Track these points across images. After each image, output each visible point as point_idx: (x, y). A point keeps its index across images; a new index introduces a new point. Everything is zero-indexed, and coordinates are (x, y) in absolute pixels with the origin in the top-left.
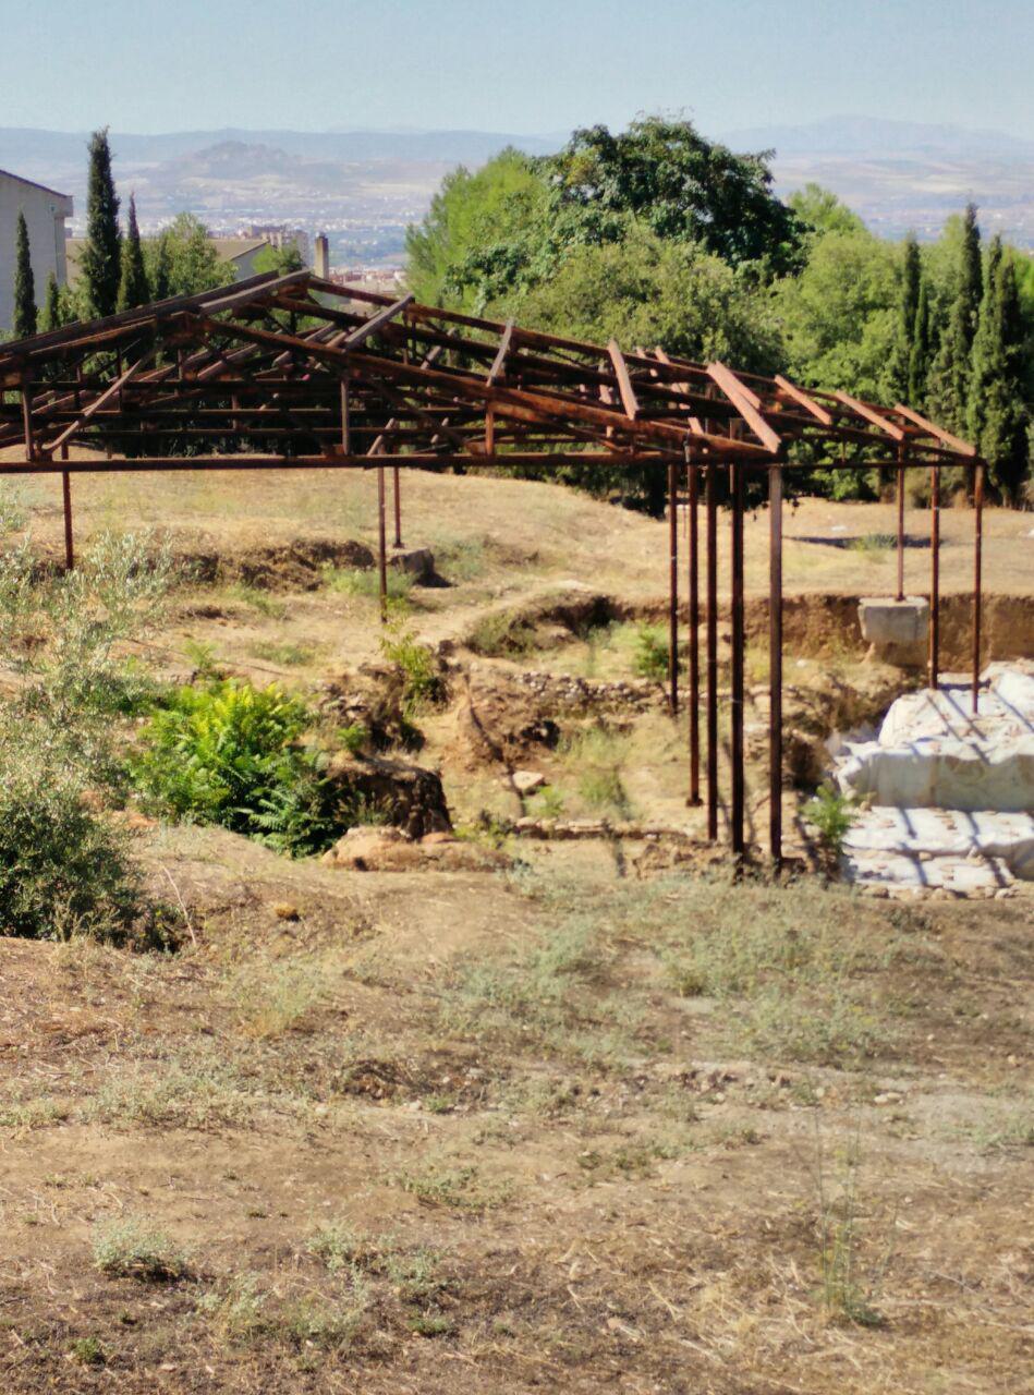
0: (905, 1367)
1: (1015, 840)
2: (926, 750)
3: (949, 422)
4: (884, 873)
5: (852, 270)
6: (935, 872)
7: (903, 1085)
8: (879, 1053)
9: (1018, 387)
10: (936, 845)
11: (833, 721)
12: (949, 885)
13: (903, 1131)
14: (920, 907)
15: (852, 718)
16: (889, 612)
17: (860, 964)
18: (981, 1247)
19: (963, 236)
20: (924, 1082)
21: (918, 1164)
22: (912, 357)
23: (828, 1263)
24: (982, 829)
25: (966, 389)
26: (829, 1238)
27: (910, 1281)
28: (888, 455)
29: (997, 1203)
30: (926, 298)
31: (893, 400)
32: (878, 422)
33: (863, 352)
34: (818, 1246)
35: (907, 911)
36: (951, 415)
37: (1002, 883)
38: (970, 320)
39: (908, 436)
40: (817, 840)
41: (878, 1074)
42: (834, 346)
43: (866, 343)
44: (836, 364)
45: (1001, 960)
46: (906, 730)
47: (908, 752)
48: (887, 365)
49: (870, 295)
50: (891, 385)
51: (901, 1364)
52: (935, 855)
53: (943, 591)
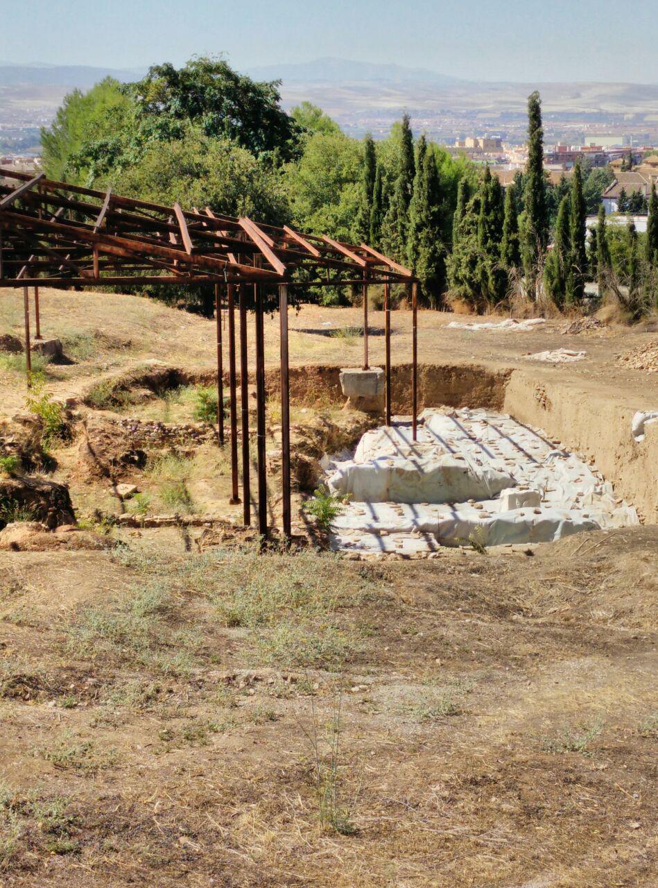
0: (371, 859)
2: (384, 465)
4: (358, 544)
5: (332, 158)
7: (369, 679)
9: (438, 232)
10: (390, 526)
12: (399, 551)
13: (369, 709)
14: (379, 565)
16: (359, 376)
18: (418, 781)
19: (401, 136)
20: (382, 677)
22: (372, 214)
23: (321, 795)
25: (406, 234)
26: (321, 780)
28: (357, 276)
30: (380, 175)
32: (351, 256)
33: (340, 210)
35: (371, 568)
36: (397, 250)
39: (369, 264)
43: (342, 204)
44: (323, 218)
45: (431, 598)
46: (371, 452)
47: (373, 466)
50: (358, 231)
51: (368, 858)
52: (390, 532)
53: (393, 363)
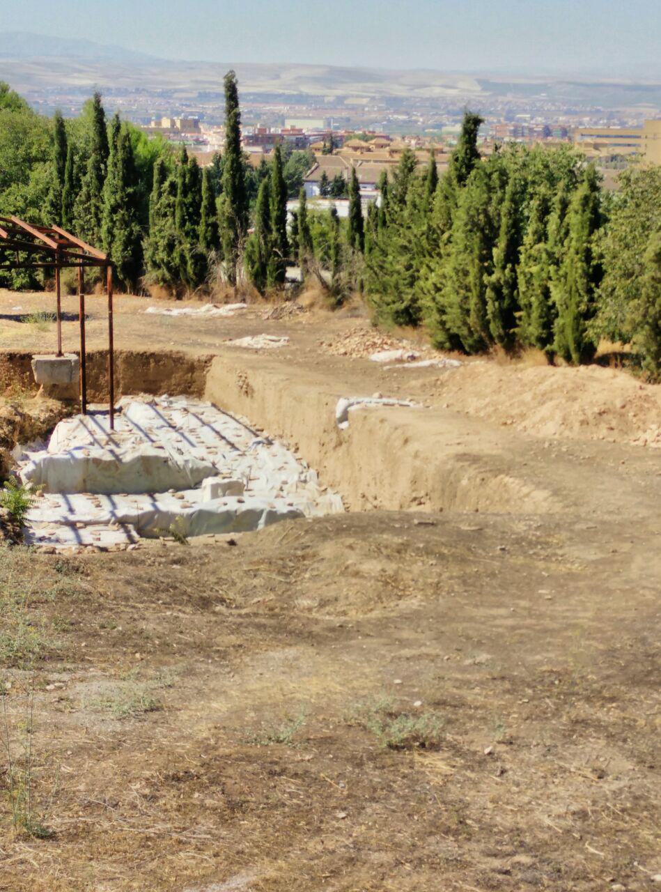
0: (68, 863)
1: (140, 512)
2: (79, 455)
3: (90, 237)
4: (53, 537)
5: (21, 135)
6: (87, 535)
7: (65, 677)
8: (48, 657)
9: (134, 214)
10: (87, 518)
11: (16, 437)
12: (97, 543)
13: (65, 707)
14: (75, 559)
15: (29, 435)
16: (52, 363)
17: (34, 598)
18: (118, 780)
19: (93, 114)
20: (79, 674)
21: (75, 729)
22: (64, 194)
23: (15, 799)
24: (119, 506)
25: (100, 216)
26: (15, 782)
27: (71, 806)
28: (50, 259)
29: (128, 750)
30: (72, 155)
31: (51, 222)
32: (42, 238)
33: (30, 190)
34: (8, 788)
35: (67, 562)
36: (91, 233)
37: (132, 541)
38: (100, 170)
39: (60, 246)
40: (6, 517)
41: (48, 671)
42: (9, 186)
43: (32, 184)
44: (12, 198)
45: (130, 591)
46: (66, 442)
47: (68, 456)
48: (46, 199)
49: (34, 152)
50: (48, 212)
51: (65, 861)
52: (87, 524)
53: (88, 349)
